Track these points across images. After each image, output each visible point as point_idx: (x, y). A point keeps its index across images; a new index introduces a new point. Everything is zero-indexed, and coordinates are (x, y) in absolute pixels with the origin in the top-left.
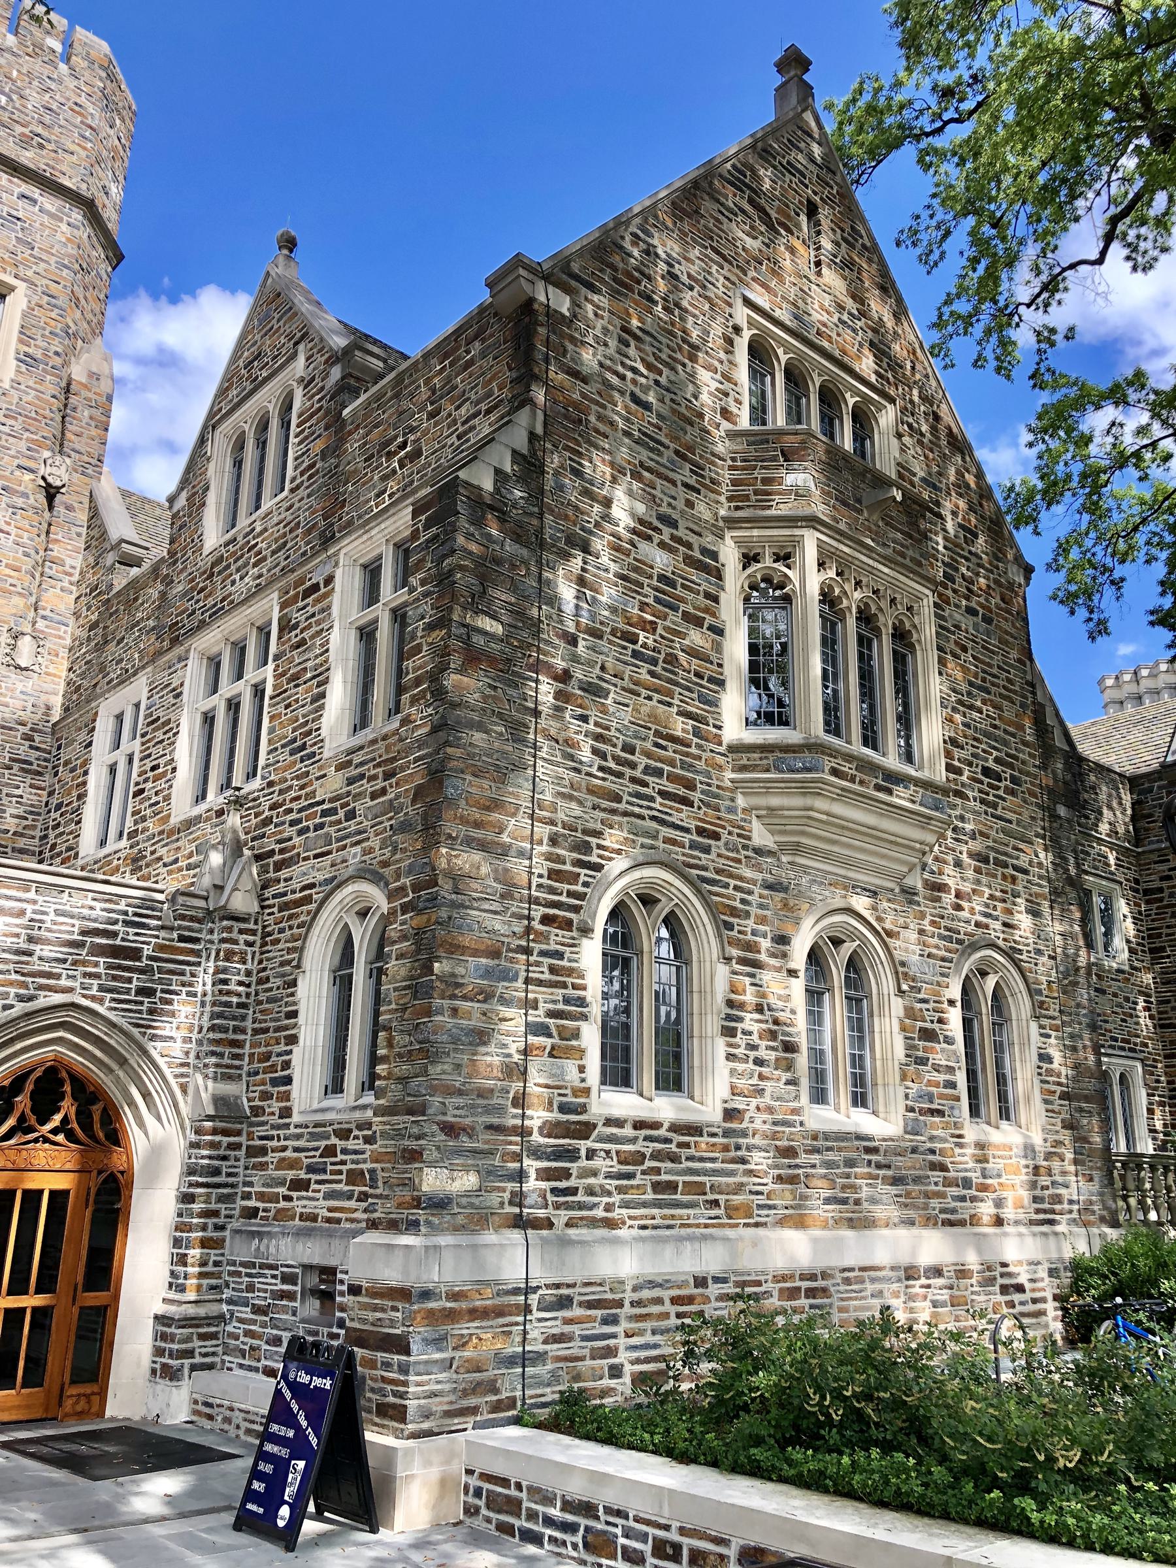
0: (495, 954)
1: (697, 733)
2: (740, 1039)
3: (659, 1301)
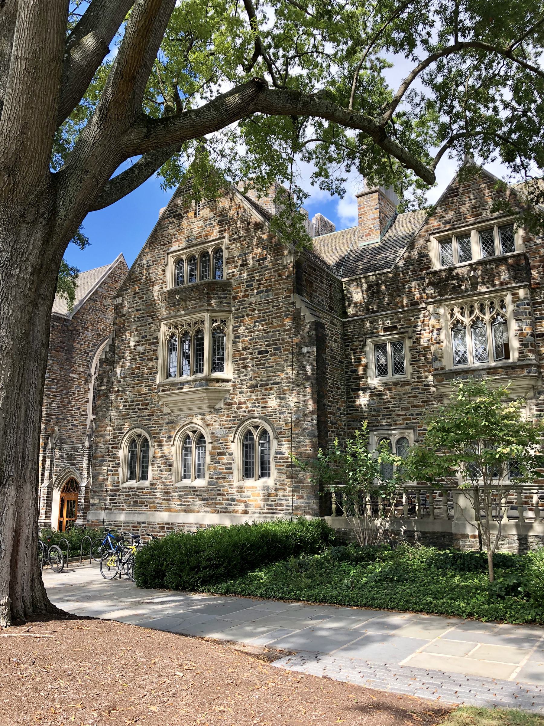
0: (103, 457)
1: (149, 390)
2: (156, 466)
3: (129, 526)
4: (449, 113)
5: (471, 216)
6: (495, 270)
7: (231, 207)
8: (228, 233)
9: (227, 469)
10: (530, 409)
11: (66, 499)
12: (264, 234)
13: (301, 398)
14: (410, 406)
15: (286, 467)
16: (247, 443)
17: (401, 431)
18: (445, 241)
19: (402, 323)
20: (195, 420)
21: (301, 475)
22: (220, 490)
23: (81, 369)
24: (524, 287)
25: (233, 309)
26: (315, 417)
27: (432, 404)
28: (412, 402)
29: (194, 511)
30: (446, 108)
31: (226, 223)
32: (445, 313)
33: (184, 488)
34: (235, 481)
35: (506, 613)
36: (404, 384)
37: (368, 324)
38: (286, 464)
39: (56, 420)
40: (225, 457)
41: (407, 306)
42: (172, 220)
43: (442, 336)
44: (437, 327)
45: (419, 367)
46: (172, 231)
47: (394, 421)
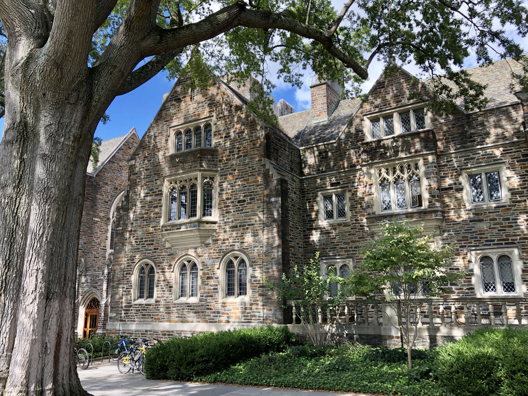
2: (160, 287)
3: (139, 334)
4: (377, 28)
5: (393, 102)
6: (411, 142)
7: (217, 94)
8: (216, 113)
9: (214, 289)
10: (437, 243)
11: (90, 314)
12: (242, 114)
13: (270, 235)
14: (350, 241)
15: (259, 287)
16: (229, 269)
17: (344, 260)
18: (374, 120)
19: (344, 180)
20: (189, 253)
21: (270, 293)
22: (208, 305)
23: (102, 214)
24: (432, 154)
25: (219, 169)
26: (280, 249)
27: (366, 240)
28: (352, 238)
29: (188, 322)
30: (375, 24)
31: (214, 106)
32: (375, 173)
33: (181, 304)
34: (220, 298)
35: (421, 391)
36: (346, 225)
37: (319, 181)
38: (258, 285)
39: (83, 254)
40: (212, 280)
41: (347, 168)
42: (174, 103)
43: (373, 190)
44: (369, 183)
45: (356, 212)
46: (174, 111)
47: (338, 252)
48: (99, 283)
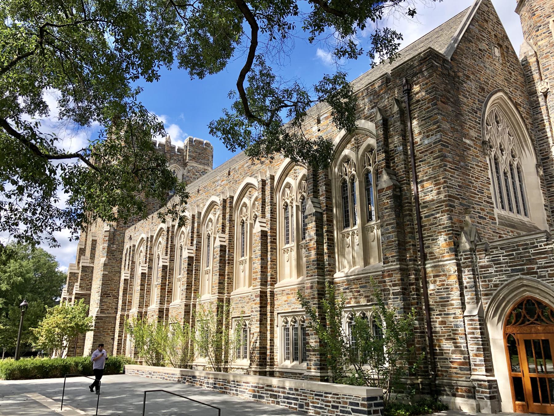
11: (519, 338)
39: (461, 207)
48: (542, 262)
